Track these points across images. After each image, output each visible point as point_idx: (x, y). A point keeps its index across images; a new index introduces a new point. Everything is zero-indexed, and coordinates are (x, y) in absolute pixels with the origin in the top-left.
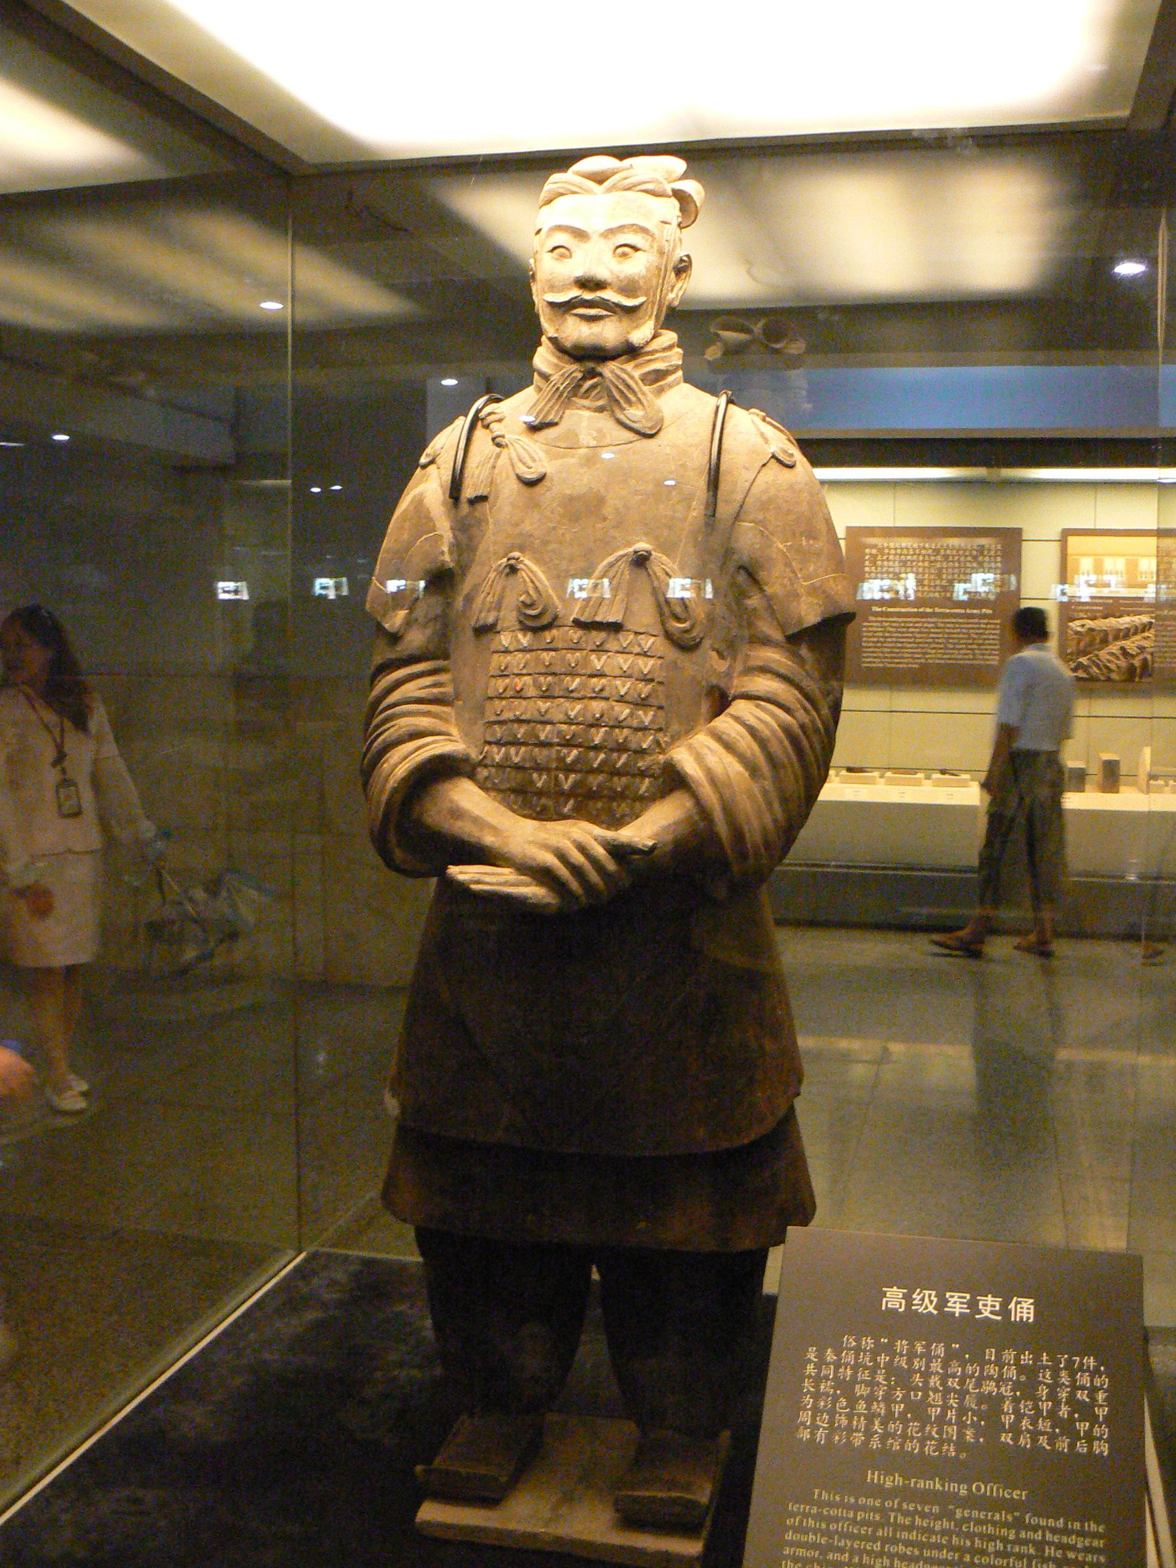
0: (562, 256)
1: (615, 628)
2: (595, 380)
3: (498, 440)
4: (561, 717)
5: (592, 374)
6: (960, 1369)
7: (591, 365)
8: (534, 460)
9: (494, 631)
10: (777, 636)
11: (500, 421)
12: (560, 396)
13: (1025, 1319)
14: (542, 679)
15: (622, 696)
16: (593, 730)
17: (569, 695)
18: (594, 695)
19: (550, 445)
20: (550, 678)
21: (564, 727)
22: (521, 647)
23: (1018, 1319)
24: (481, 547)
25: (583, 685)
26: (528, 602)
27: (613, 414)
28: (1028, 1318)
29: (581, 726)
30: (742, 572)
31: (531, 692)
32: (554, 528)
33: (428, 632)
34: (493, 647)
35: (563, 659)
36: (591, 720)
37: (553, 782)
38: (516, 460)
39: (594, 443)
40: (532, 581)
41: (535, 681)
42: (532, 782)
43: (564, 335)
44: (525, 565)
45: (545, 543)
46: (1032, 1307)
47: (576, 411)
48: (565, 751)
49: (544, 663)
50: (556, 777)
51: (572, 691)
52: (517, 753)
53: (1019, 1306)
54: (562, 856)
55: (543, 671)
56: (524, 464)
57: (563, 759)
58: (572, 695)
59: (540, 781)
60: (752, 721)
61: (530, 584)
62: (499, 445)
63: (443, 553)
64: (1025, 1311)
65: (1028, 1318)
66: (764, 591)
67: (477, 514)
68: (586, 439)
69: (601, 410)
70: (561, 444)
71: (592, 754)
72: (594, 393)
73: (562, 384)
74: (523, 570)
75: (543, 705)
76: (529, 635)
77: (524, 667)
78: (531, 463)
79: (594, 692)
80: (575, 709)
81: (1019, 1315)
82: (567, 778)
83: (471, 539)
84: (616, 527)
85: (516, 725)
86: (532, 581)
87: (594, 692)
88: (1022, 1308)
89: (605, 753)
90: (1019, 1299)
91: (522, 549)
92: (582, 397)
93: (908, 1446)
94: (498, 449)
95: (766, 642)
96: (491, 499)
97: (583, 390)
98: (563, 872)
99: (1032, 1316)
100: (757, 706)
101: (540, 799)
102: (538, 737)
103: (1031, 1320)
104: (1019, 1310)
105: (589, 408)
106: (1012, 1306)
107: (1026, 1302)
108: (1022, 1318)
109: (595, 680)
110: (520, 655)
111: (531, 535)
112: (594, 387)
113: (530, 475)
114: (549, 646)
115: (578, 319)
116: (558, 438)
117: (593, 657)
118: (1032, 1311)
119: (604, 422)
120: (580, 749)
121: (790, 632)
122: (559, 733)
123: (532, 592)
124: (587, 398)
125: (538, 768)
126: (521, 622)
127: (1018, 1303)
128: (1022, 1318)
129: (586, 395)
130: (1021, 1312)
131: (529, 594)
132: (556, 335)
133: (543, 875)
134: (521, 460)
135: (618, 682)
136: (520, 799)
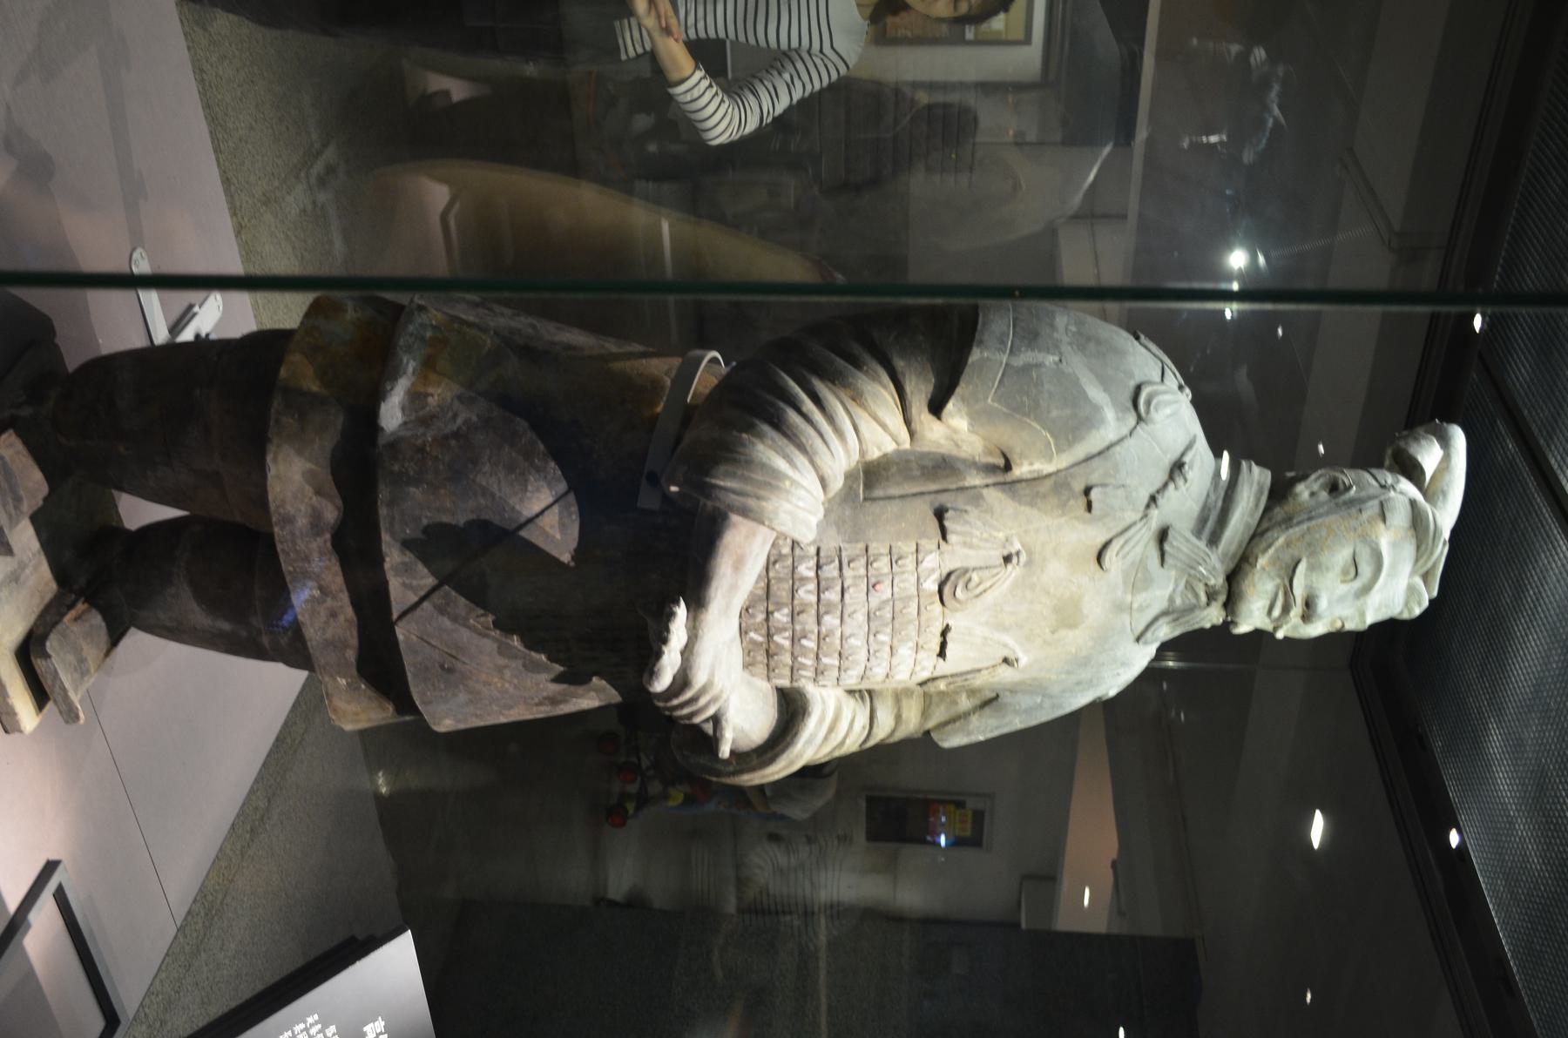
0: (1345, 572)
1: (942, 654)
2: (1203, 598)
3: (1153, 506)
4: (848, 631)
5: (1211, 596)
7: (1222, 598)
8: (1124, 557)
9: (941, 541)
10: (930, 725)
11: (1176, 488)
12: (1192, 568)
14: (889, 608)
15: (871, 669)
16: (837, 655)
17: (872, 633)
18: (871, 651)
19: (1141, 565)
20: (889, 616)
21: (838, 634)
22: (922, 580)
24: (1035, 512)
25: (883, 643)
26: (971, 585)
27: (1164, 613)
29: (839, 648)
30: (994, 695)
31: (875, 601)
32: (1048, 593)
33: (943, 441)
34: (924, 543)
35: (910, 622)
36: (845, 654)
37: (781, 626)
38: (1127, 535)
39: (1135, 606)
40: (991, 587)
41: (885, 602)
42: (779, 606)
43: (1256, 577)
44: (1011, 573)
45: (1033, 587)
47: (1173, 581)
48: (814, 637)
49: (904, 608)
50: (785, 629)
51: (875, 635)
52: (809, 592)
54: (703, 690)
55: (897, 609)
56: (1122, 547)
57: (805, 637)
58: (871, 637)
59: (781, 617)
60: (848, 741)
61: (988, 584)
62: (1148, 506)
63: (1031, 464)
66: (974, 713)
67: (1072, 502)
68: (1140, 599)
69: (1171, 600)
70: (1139, 575)
71: (812, 656)
72: (1190, 596)
73: (1205, 569)
74: (1006, 572)
75: (861, 617)
76: (936, 588)
77: (900, 588)
78: (1120, 555)
79: (875, 652)
80: (857, 642)
82: (785, 638)
83: (1044, 497)
84: (1045, 642)
85: (838, 588)
86: (991, 587)
87: (875, 652)
89: (812, 665)
91: (1029, 563)
92: (1187, 582)
94: (1142, 508)
95: (925, 714)
96: (1087, 515)
97: (1195, 583)
98: (688, 695)
100: (864, 728)
101: (762, 612)
102: (827, 613)
105: (1174, 591)
109: (888, 649)
110: (913, 579)
111: (1042, 571)
112: (1196, 596)
113: (1109, 556)
114: (922, 608)
115: (1271, 595)
116: (1146, 570)
117: (911, 644)
119: (1159, 605)
120: (816, 648)
121: (934, 735)
122: (830, 634)
123: (981, 588)
124: (1186, 587)
125: (793, 616)
126: (949, 575)
129: (1188, 587)
131: (978, 585)
132: (1258, 566)
133: (682, 681)
134: (1126, 542)
135: (885, 664)
136: (761, 592)
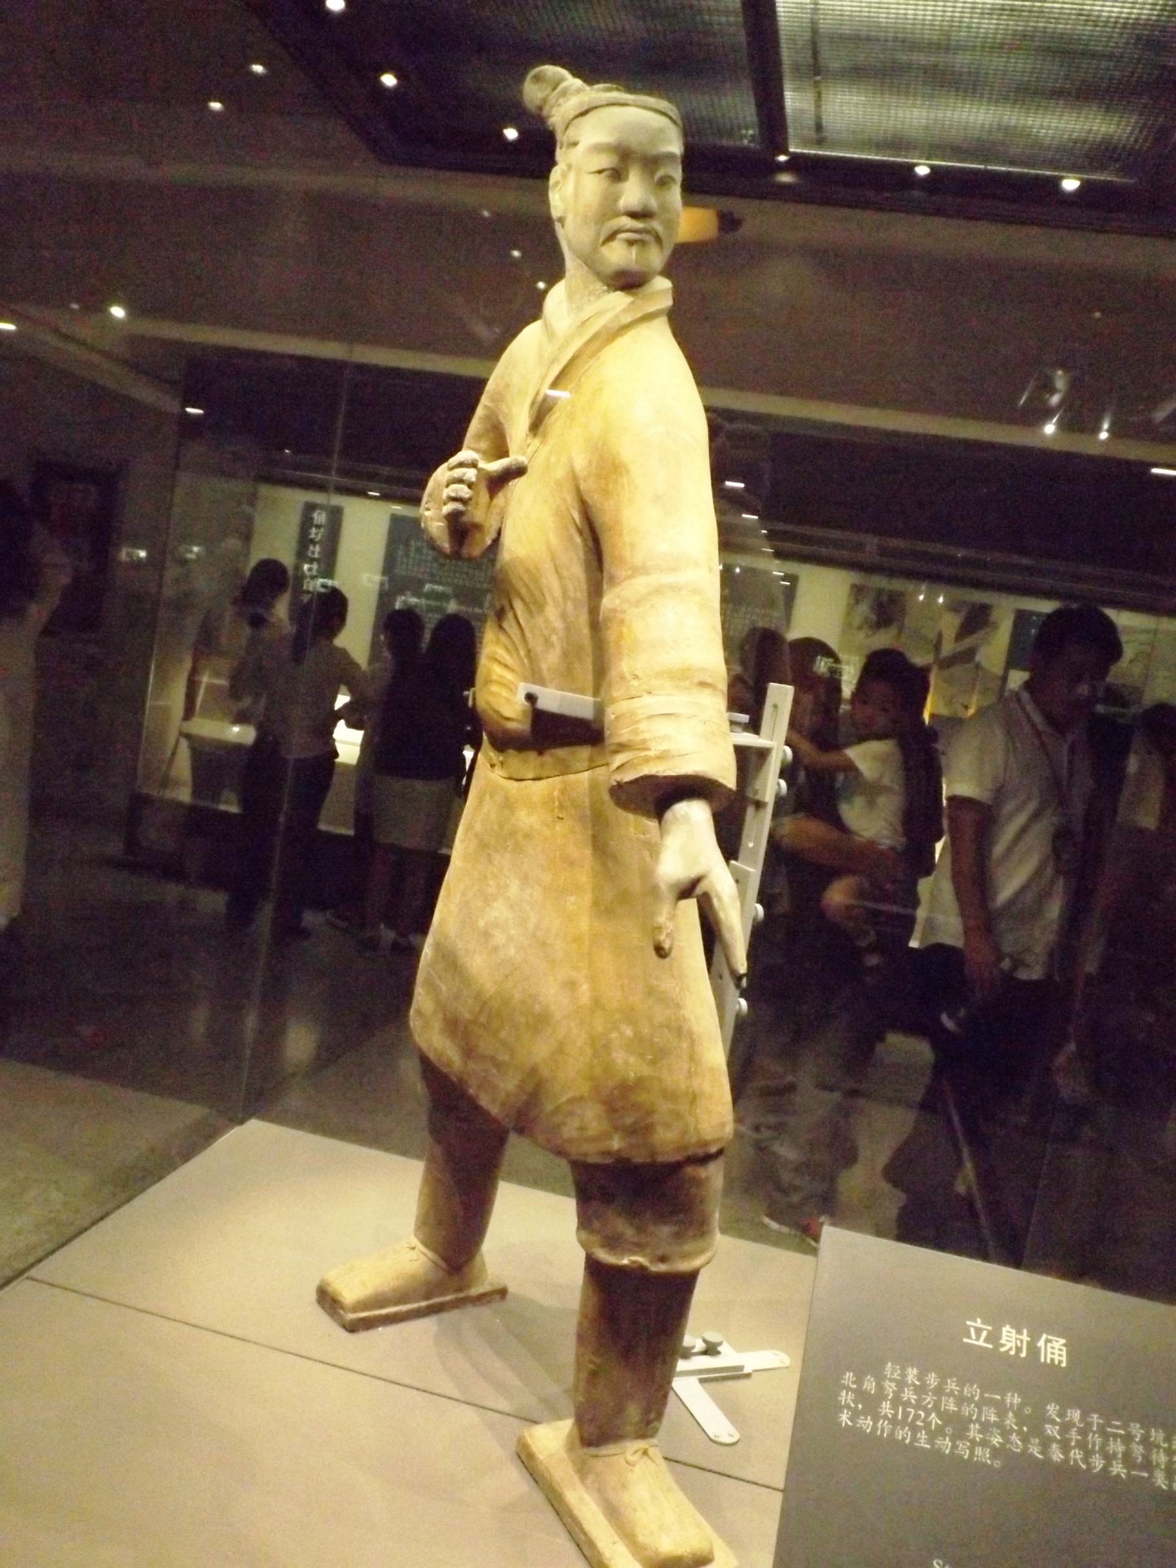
6: (968, 1451)
13: (1056, 1362)
23: (1049, 1361)
28: (1060, 1362)
46: (1064, 1349)
53: (1049, 1345)
64: (1056, 1352)
65: (1060, 1362)
81: (1049, 1356)
88: (1053, 1348)
90: (1050, 1337)
93: (899, 1434)
99: (1064, 1359)
103: (1064, 1365)
104: (1049, 1350)
106: (1041, 1343)
107: (1057, 1341)
108: (1052, 1360)
118: (1064, 1353)
127: (1048, 1341)
128: (1052, 1360)
130: (1053, 1354)
